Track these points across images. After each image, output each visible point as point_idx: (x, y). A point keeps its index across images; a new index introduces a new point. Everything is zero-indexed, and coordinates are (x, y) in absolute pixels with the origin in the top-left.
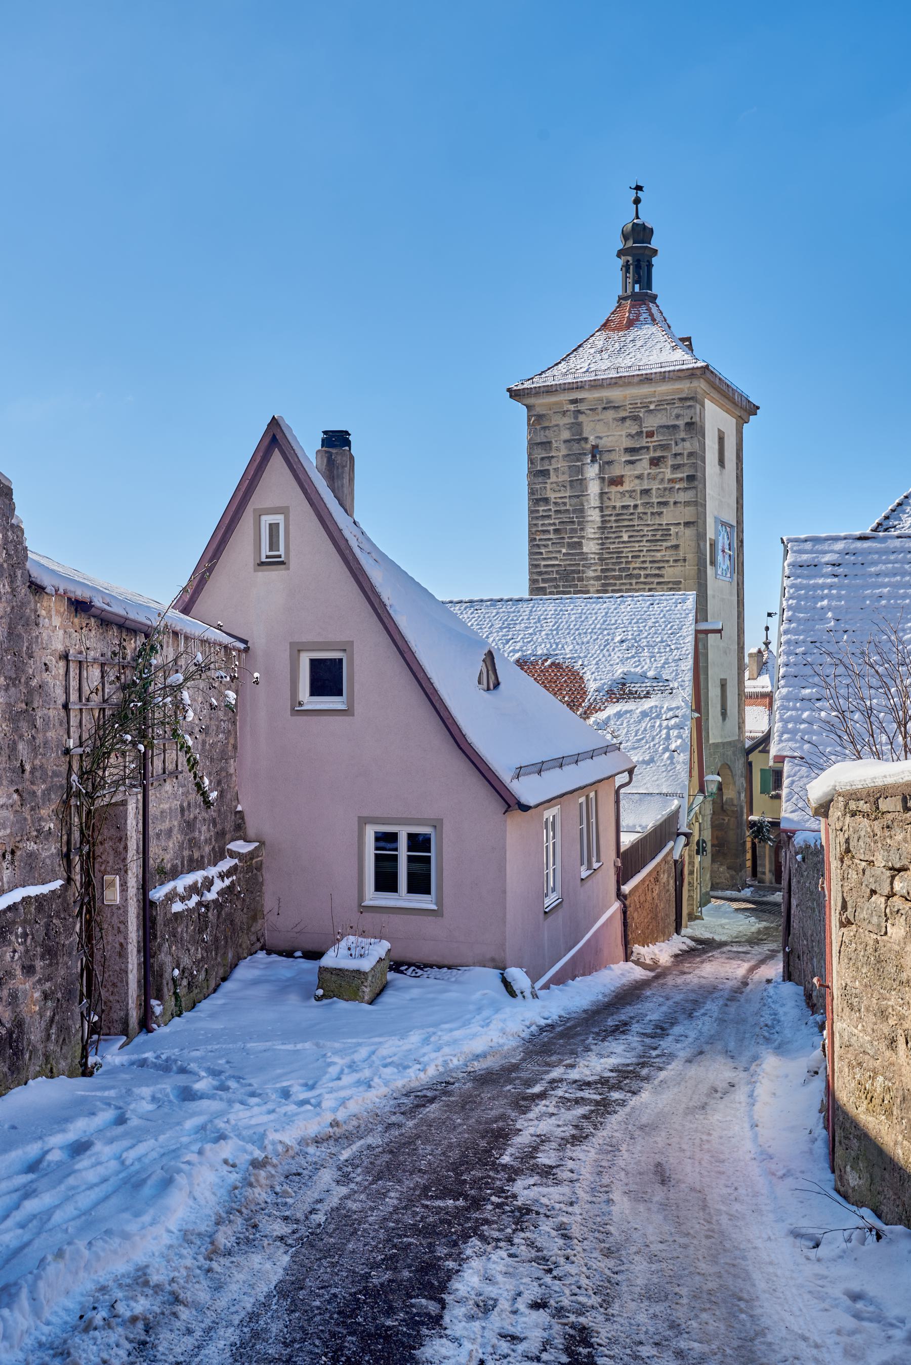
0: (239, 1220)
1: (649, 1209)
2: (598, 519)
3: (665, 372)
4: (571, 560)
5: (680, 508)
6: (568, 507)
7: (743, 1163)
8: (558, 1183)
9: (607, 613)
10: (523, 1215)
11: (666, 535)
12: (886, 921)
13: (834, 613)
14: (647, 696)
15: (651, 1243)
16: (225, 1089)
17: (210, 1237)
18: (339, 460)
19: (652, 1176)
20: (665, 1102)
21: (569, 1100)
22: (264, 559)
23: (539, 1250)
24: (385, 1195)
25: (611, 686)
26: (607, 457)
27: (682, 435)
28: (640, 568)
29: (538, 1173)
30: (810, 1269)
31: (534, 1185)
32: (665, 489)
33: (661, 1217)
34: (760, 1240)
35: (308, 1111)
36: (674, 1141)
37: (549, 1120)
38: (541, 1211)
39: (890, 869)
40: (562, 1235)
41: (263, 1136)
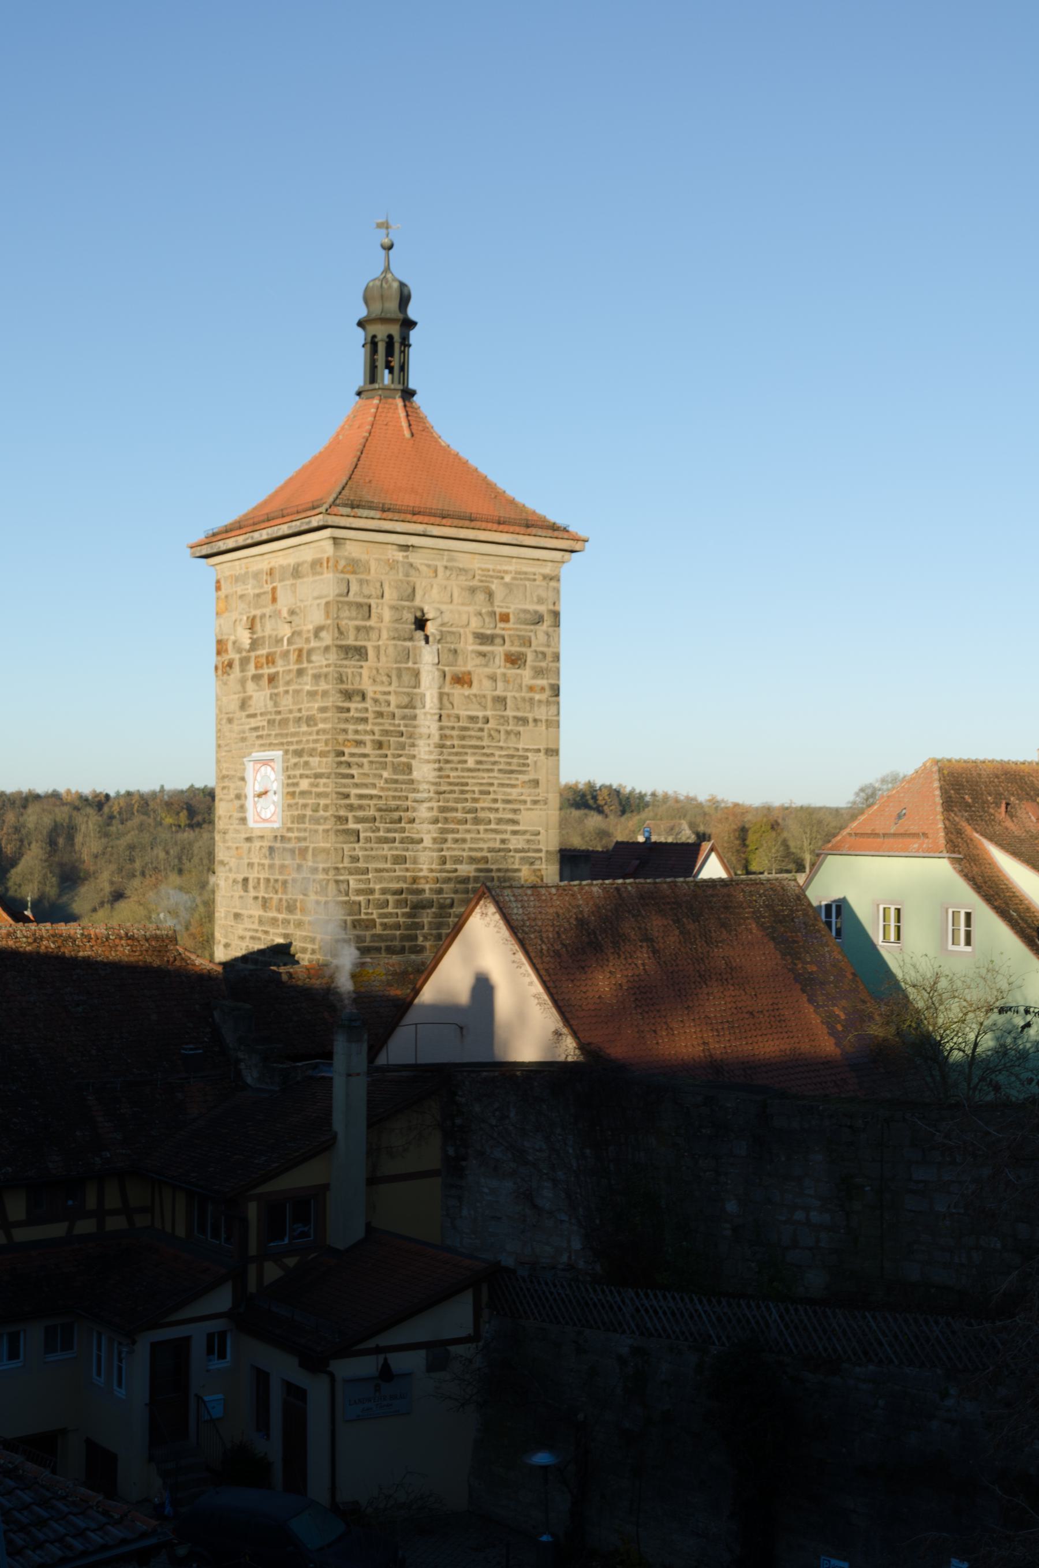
4: (396, 790)
6: (392, 708)
28: (490, 809)
32: (524, 699)
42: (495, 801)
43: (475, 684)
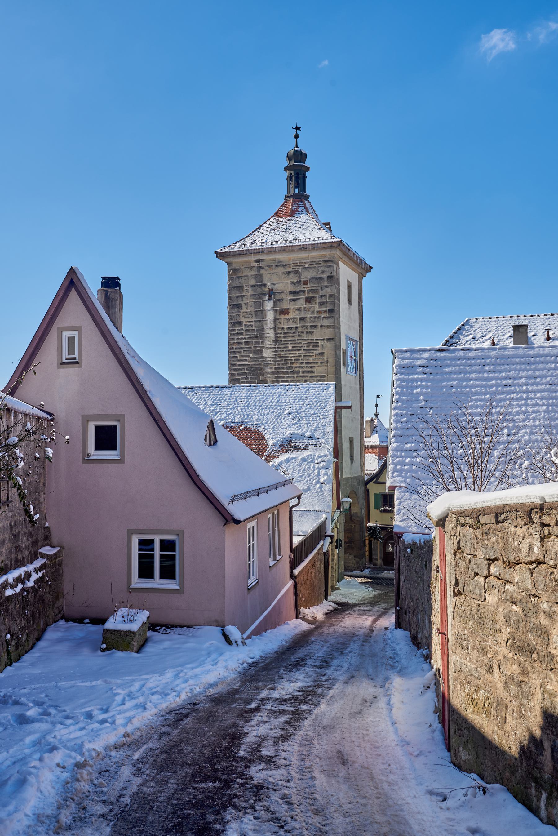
0: (73, 805)
1: (338, 782)
2: (273, 336)
3: (315, 244)
5: (325, 329)
7: (391, 748)
8: (278, 767)
9: (279, 396)
10: (259, 790)
11: (316, 346)
12: (485, 592)
13: (424, 397)
14: (306, 448)
15: (343, 804)
16: (49, 714)
17: (55, 817)
18: (112, 296)
19: (336, 759)
20: (336, 711)
21: (275, 712)
22: (64, 360)
23: (273, 813)
24: (167, 782)
25: (282, 442)
26: (278, 297)
27: (326, 283)
28: (299, 367)
29: (263, 761)
30: (443, 815)
31: (262, 770)
32: (315, 317)
33: (346, 786)
34: (409, 798)
35: (107, 727)
36: (347, 735)
37: (264, 726)
38: (270, 786)
39: (487, 560)
40: (286, 802)
41: (82, 745)
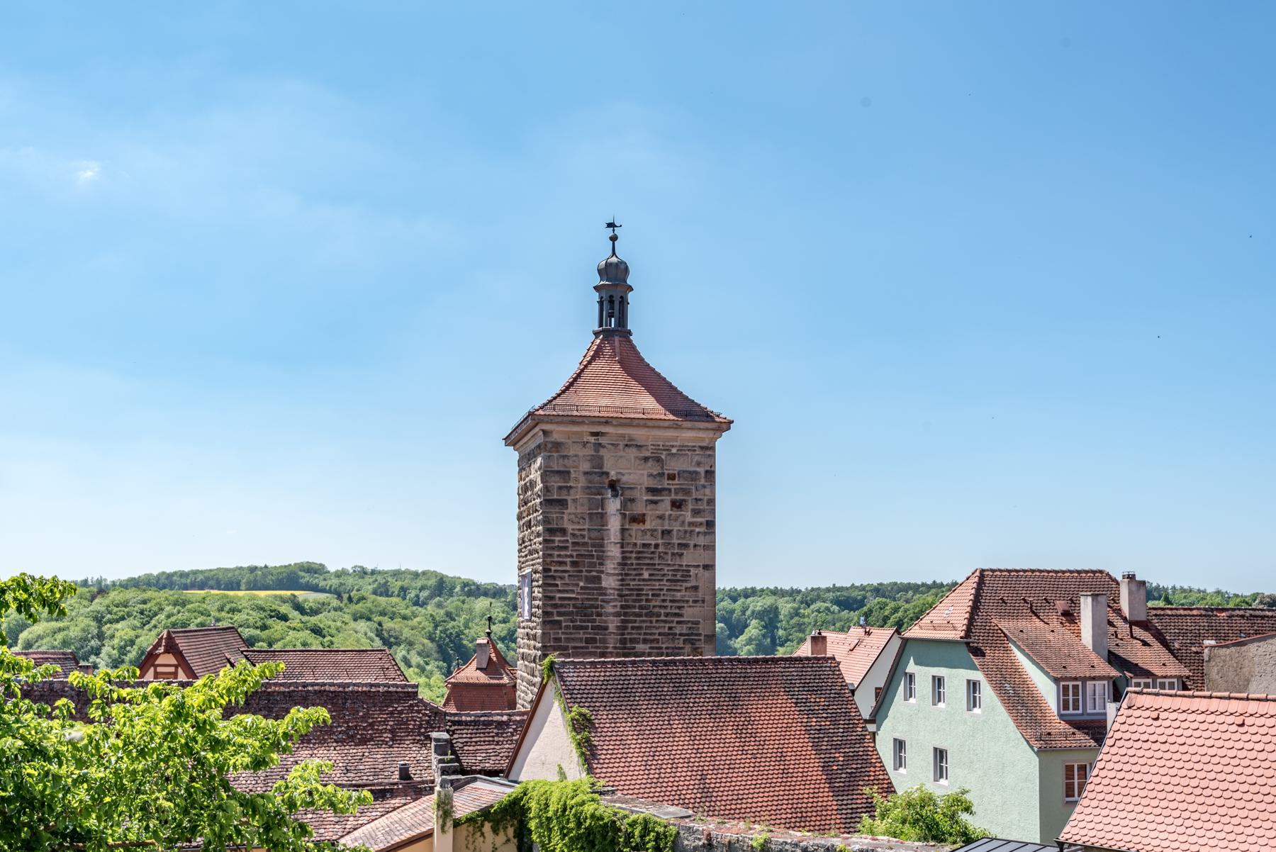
6: (586, 540)
11: (686, 576)
26: (628, 494)
27: (703, 481)
32: (686, 532)
42: (664, 601)
43: (648, 523)
